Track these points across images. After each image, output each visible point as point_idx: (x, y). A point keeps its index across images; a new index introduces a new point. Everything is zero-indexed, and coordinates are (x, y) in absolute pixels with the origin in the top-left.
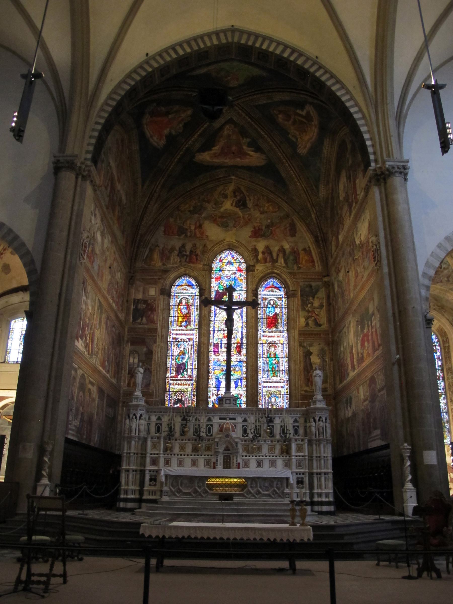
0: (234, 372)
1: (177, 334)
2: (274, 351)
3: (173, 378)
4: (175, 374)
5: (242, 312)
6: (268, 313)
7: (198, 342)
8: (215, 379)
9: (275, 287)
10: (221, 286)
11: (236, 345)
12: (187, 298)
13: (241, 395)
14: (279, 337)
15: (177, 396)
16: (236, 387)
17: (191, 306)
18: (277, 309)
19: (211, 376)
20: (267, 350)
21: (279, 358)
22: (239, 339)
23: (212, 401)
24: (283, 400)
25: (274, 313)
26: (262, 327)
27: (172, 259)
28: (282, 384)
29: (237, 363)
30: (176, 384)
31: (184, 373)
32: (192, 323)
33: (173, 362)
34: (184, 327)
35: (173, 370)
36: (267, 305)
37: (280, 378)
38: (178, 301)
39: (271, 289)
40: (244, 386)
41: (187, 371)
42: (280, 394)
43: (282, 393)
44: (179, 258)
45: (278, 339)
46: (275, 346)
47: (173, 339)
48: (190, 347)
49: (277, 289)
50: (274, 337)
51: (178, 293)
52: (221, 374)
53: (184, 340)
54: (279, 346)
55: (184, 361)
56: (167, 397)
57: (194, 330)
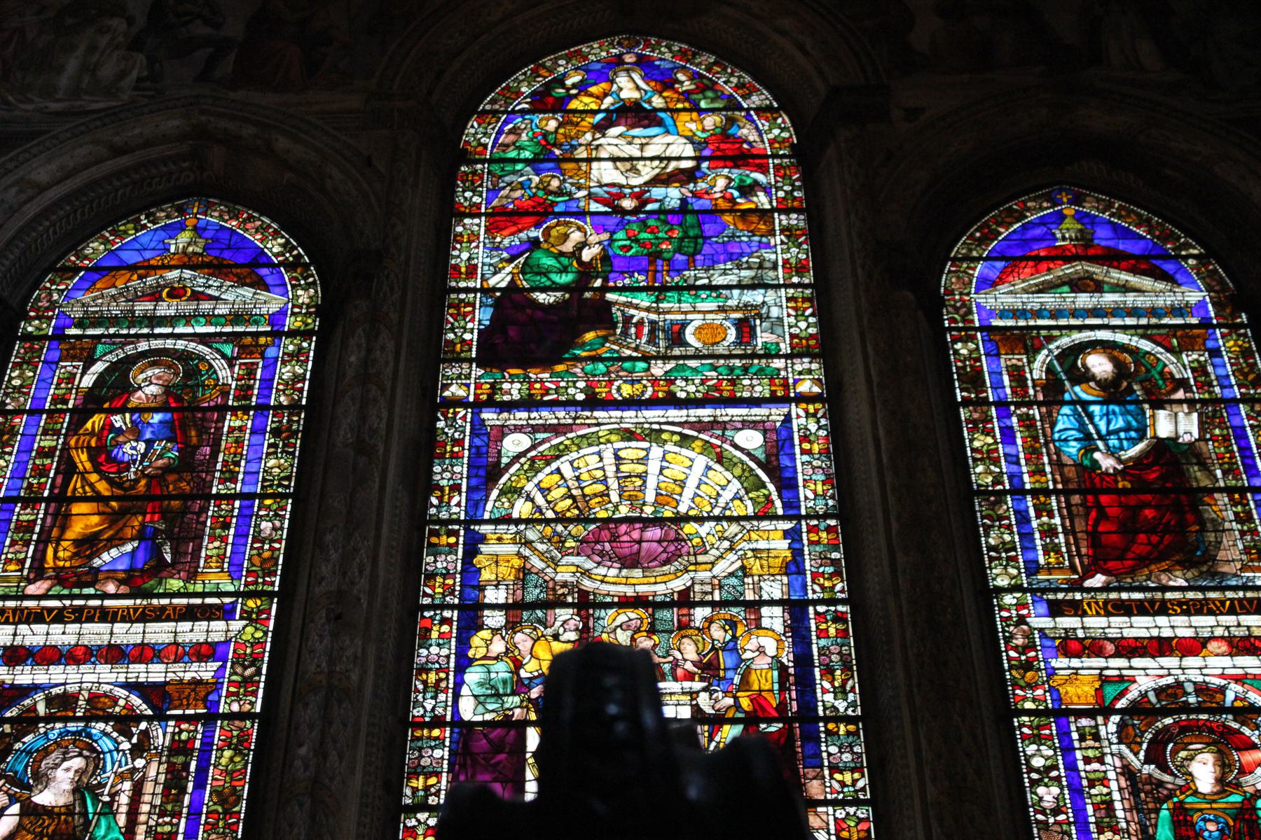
2: (1224, 784)
6: (1073, 449)
7: (266, 719)
9: (1112, 258)
10: (548, 262)
12: (185, 356)
17: (223, 409)
18: (1162, 415)
20: (1127, 771)
22: (765, 679)
25: (1140, 446)
26: (1033, 568)
27: (72, 65)
32: (209, 548)
36: (1053, 392)
38: (88, 381)
39: (1068, 270)
44: (141, 58)
48: (155, 770)
49: (1135, 271)
50: (1194, 646)
51: (97, 321)
53: (99, 707)
57: (226, 613)
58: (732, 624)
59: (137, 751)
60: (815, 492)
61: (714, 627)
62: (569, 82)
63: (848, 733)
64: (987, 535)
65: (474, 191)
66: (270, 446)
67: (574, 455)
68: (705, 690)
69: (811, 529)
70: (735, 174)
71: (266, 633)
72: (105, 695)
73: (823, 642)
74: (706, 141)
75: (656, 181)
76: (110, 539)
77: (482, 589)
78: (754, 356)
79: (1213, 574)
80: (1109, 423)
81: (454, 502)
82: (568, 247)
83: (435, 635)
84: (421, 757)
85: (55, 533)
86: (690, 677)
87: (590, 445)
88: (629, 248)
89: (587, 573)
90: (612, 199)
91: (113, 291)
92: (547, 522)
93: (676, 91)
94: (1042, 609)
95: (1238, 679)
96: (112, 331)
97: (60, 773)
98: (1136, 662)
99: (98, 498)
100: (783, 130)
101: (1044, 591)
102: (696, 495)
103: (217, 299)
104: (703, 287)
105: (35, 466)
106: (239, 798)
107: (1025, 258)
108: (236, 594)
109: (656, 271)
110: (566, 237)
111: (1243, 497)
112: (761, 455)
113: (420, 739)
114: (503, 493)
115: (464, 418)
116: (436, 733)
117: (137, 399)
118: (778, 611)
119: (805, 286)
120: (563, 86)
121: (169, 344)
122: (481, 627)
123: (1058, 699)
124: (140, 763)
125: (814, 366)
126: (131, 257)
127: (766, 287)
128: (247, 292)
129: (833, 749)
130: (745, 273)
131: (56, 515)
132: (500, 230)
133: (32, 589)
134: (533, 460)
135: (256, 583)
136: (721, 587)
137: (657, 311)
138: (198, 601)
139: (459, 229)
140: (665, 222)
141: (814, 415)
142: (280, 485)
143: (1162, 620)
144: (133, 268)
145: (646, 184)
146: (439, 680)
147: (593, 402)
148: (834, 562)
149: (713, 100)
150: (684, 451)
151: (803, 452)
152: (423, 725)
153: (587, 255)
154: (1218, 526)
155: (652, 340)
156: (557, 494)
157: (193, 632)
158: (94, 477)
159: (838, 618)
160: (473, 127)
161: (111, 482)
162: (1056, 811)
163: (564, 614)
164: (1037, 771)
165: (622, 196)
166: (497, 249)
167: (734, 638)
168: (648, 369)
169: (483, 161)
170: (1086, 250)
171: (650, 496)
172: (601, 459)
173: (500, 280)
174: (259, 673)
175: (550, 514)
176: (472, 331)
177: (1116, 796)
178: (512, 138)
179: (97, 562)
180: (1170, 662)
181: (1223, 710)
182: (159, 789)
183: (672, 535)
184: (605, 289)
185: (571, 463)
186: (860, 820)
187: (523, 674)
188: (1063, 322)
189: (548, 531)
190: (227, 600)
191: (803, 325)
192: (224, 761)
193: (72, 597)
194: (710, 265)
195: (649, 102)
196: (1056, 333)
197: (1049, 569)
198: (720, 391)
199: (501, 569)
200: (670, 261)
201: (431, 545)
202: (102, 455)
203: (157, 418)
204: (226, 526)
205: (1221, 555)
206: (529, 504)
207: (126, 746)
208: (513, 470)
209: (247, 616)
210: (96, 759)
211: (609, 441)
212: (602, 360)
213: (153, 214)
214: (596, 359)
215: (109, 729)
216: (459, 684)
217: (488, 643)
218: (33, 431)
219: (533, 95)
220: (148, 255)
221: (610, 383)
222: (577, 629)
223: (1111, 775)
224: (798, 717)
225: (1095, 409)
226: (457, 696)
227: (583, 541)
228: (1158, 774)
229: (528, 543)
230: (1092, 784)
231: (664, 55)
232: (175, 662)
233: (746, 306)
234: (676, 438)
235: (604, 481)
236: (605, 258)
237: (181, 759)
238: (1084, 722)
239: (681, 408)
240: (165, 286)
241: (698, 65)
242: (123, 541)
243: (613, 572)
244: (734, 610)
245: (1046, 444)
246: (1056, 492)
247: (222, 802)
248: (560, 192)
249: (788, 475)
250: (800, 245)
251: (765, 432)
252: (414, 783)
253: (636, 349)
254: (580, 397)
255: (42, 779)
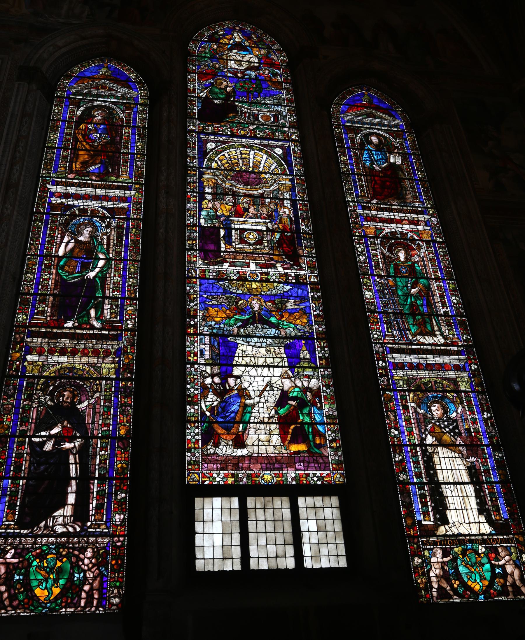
0: (282, 316)
1: (67, 196)
3: (43, 330)
4: (52, 315)
5: (287, 153)
6: (368, 163)
7: (143, 220)
8: (211, 335)
9: (378, 109)
10: (217, 90)
11: (277, 236)
13: (317, 393)
14: (415, 222)
15: (51, 394)
16: (292, 367)
17: (122, 126)
18: (391, 156)
19: (195, 326)
20: (382, 254)
21: (427, 278)
22: (286, 221)
23: (203, 414)
24: (472, 412)
26: (358, 196)
28: (455, 360)
29: (288, 288)
30: (52, 352)
31: (89, 314)
32: (122, 169)
33: (46, 275)
34: (94, 178)
35: (43, 301)
37: (445, 338)
38: (79, 113)
39: (366, 110)
40: (324, 362)
41: (99, 308)
42: (458, 391)
43: (463, 386)
45: (413, 227)
46: (408, 249)
47: (52, 206)
52: (232, 321)
53: (94, 213)
54: (419, 248)
55: (92, 274)
56: (12, 395)
57: (130, 189)
58: (276, 204)
59: (108, 227)
60: (297, 168)
61: (271, 205)
62: (220, 33)
63: (309, 238)
64: (345, 186)
65: (193, 65)
66: (138, 139)
67: (228, 151)
68: (269, 222)
69: (297, 179)
70: (271, 69)
71: (142, 196)
72: (96, 210)
73: (301, 212)
74: (262, 58)
75: (247, 69)
76: (91, 163)
77: (205, 188)
78: (279, 126)
79: (405, 202)
80: (377, 157)
81: (194, 161)
82: (223, 86)
83: (192, 200)
84: (190, 235)
85: (74, 159)
86: (265, 218)
87: (233, 148)
88: (241, 89)
89: (234, 186)
90: (235, 72)
91: (84, 85)
92: (222, 170)
93: (252, 41)
94: (360, 208)
95: (411, 231)
96: (85, 98)
97: (85, 231)
98: (385, 225)
99: (86, 150)
100: (284, 57)
101: (361, 203)
102: (264, 166)
103: (117, 91)
104: (263, 104)
105: (66, 139)
106: (139, 243)
107: (355, 106)
108: (132, 183)
109: (249, 97)
110: (222, 83)
111: (413, 181)
112: (281, 156)
113: (190, 230)
114: (208, 160)
115: (195, 136)
116: (194, 228)
117: (95, 120)
118: (289, 202)
119: (293, 107)
120: (218, 35)
121: (103, 103)
122: (205, 199)
123: (364, 233)
124: (108, 230)
125: (296, 131)
126: (88, 74)
127: (282, 106)
128: (126, 90)
129: (305, 242)
130: (275, 101)
131: (74, 154)
132: (202, 79)
133: (69, 176)
134: (216, 151)
135: (137, 180)
136: (273, 194)
137: (250, 109)
138: (121, 184)
139: (189, 77)
140: (251, 82)
141: (297, 146)
142: (142, 151)
143: (391, 214)
144: (89, 78)
145: (245, 69)
146: (194, 214)
147: (233, 135)
148: (304, 189)
149: (263, 45)
150: (260, 153)
151: (294, 156)
152: (190, 226)
153: (228, 89)
154: (406, 189)
155: (249, 118)
156: (224, 162)
157: (120, 193)
158: (84, 143)
159: (305, 205)
160: (191, 44)
161: (90, 145)
162: (364, 263)
163: (228, 197)
164: (359, 252)
165: (238, 72)
166: (201, 85)
167: (277, 208)
168: (248, 127)
169: (195, 56)
170: (370, 105)
171: (251, 165)
172: (236, 153)
173: (203, 94)
174: (141, 207)
175: (222, 168)
176: (195, 110)
177: (380, 260)
178: (203, 49)
179: (89, 170)
180: (393, 225)
181: (407, 239)
182: (115, 239)
183: (258, 177)
184: (234, 101)
185: (228, 153)
186: (313, 262)
187: (218, 214)
188: (365, 126)
189: (222, 172)
190: (129, 185)
191: (292, 118)
192: (133, 232)
193: (82, 180)
194: (265, 97)
195: (244, 43)
196: (363, 129)
197: (362, 197)
198: (270, 136)
199: (209, 182)
200: (253, 95)
201: (188, 174)
202: (86, 136)
203: (102, 127)
204: (127, 162)
205: (407, 197)
206: (216, 164)
207: (104, 225)
208: (211, 153)
209: (135, 189)
210: (95, 228)
211: (238, 148)
212: (235, 123)
213: (93, 61)
214: (233, 122)
215: (98, 220)
216: (200, 215)
217: (207, 204)
218: (64, 127)
219: (208, 36)
220: (93, 74)
221: (238, 130)
222: (232, 202)
223: (379, 254)
224: (295, 232)
225: (374, 152)
226: (199, 219)
227: (233, 176)
228: (390, 255)
229: (217, 176)
230: (374, 257)
231: (248, 28)
232: (116, 202)
233: (276, 110)
234: (257, 148)
235: (238, 159)
236: (234, 91)
237: (120, 230)
238: (371, 240)
239: (258, 140)
240: (100, 85)
241: (258, 33)
242: (96, 164)
243: (242, 186)
244: (276, 201)
245: (361, 161)
246: (363, 175)
247: (134, 243)
248: (219, 69)
249: (290, 163)
250: (290, 94)
251: (283, 149)
252: (189, 242)
253: (244, 120)
254: (229, 133)
255: (81, 233)
